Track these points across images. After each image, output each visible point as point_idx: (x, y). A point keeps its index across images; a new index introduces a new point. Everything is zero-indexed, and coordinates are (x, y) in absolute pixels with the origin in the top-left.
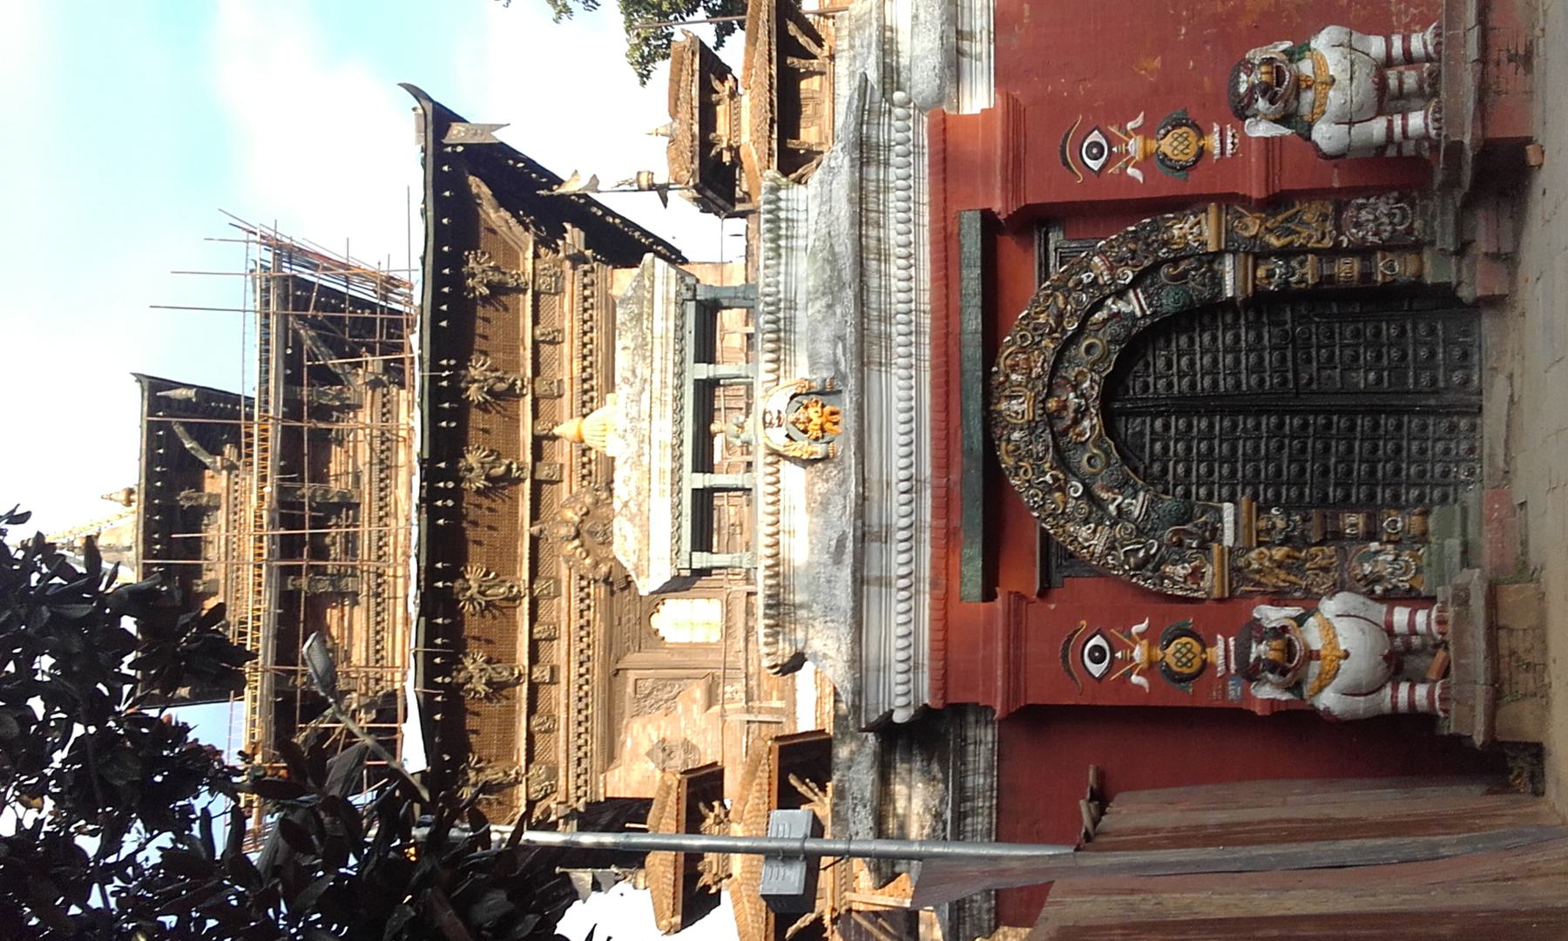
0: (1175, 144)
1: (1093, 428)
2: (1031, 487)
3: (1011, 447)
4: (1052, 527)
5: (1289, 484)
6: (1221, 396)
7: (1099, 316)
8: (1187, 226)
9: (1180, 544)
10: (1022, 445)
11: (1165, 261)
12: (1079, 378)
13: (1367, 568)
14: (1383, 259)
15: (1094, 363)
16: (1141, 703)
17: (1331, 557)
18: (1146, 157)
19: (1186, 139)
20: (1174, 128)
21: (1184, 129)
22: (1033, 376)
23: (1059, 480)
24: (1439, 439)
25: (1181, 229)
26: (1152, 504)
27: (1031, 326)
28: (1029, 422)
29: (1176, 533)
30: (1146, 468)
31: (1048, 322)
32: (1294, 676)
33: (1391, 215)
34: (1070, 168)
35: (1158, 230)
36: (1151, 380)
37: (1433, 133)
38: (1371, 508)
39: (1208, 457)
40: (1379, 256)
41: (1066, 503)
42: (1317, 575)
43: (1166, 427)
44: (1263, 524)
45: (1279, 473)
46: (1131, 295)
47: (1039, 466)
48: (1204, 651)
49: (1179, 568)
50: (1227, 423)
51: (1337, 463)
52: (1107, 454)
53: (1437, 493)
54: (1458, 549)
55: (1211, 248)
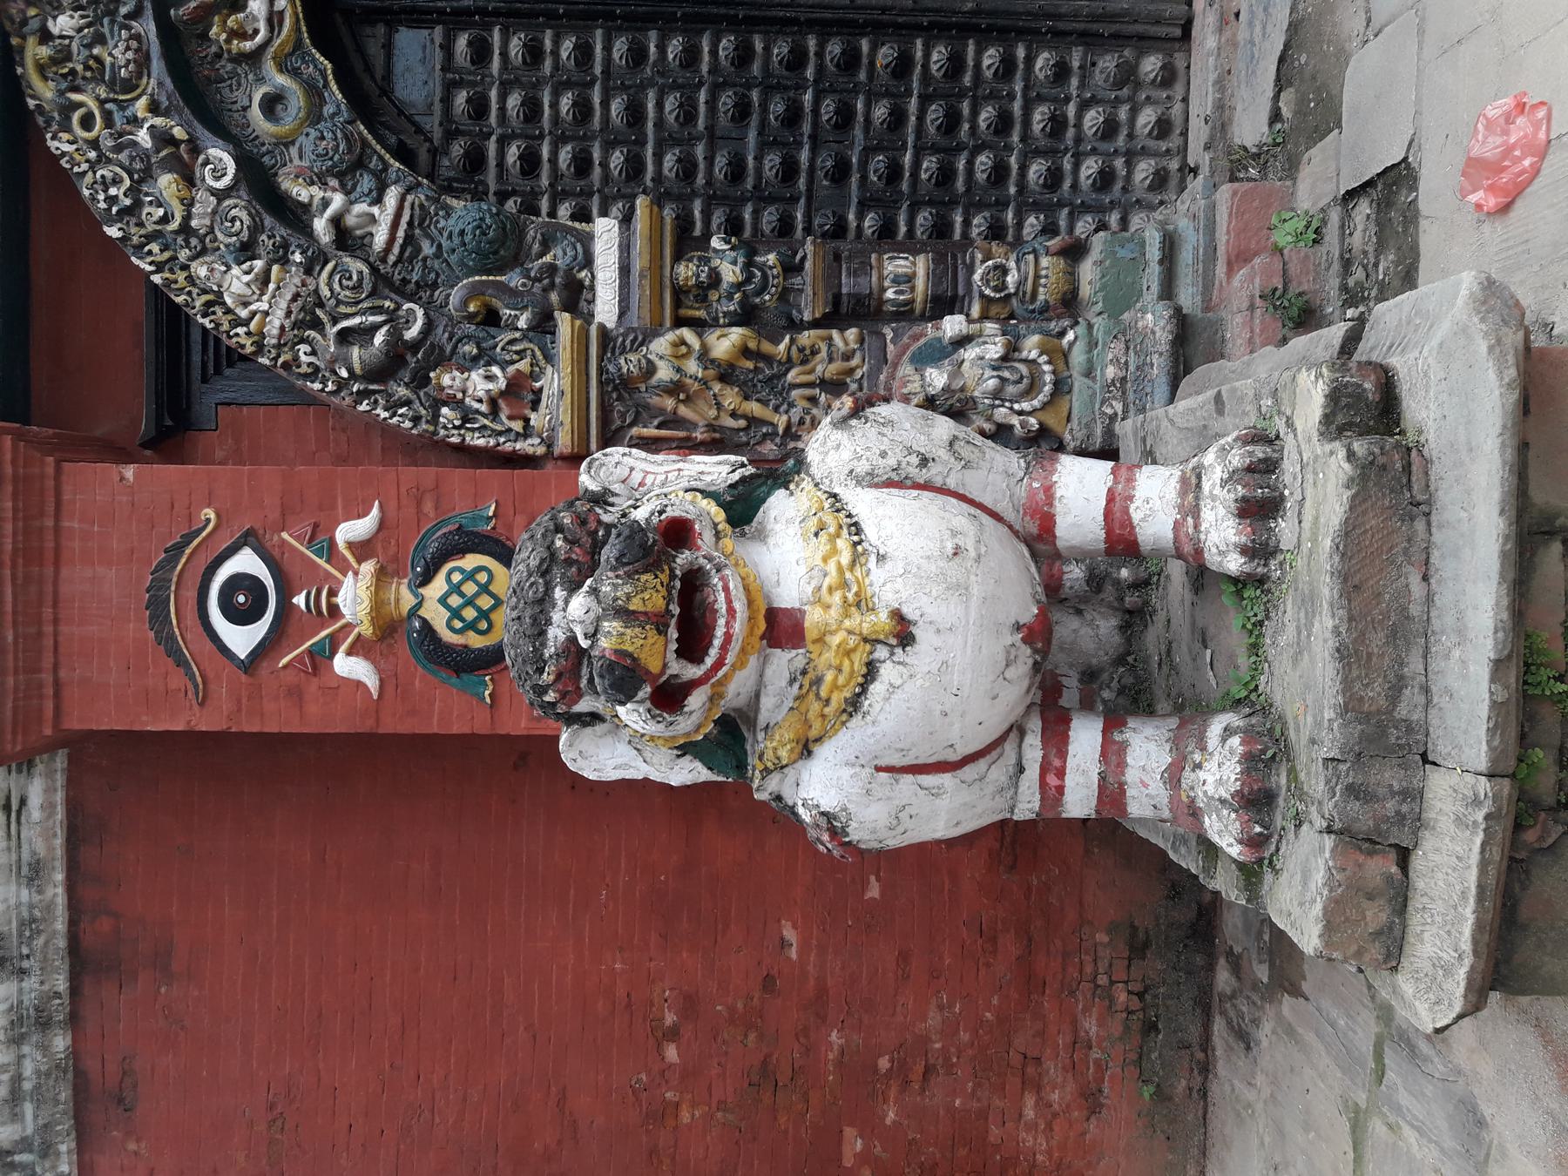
2: (102, 160)
3: (45, 52)
5: (762, 198)
9: (491, 318)
16: (366, 726)
17: (847, 357)
23: (173, 142)
29: (475, 292)
30: (434, 152)
32: (713, 699)
41: (189, 204)
42: (813, 400)
43: (481, 52)
44: (686, 271)
45: (737, 171)
51: (868, 152)
52: (315, 94)
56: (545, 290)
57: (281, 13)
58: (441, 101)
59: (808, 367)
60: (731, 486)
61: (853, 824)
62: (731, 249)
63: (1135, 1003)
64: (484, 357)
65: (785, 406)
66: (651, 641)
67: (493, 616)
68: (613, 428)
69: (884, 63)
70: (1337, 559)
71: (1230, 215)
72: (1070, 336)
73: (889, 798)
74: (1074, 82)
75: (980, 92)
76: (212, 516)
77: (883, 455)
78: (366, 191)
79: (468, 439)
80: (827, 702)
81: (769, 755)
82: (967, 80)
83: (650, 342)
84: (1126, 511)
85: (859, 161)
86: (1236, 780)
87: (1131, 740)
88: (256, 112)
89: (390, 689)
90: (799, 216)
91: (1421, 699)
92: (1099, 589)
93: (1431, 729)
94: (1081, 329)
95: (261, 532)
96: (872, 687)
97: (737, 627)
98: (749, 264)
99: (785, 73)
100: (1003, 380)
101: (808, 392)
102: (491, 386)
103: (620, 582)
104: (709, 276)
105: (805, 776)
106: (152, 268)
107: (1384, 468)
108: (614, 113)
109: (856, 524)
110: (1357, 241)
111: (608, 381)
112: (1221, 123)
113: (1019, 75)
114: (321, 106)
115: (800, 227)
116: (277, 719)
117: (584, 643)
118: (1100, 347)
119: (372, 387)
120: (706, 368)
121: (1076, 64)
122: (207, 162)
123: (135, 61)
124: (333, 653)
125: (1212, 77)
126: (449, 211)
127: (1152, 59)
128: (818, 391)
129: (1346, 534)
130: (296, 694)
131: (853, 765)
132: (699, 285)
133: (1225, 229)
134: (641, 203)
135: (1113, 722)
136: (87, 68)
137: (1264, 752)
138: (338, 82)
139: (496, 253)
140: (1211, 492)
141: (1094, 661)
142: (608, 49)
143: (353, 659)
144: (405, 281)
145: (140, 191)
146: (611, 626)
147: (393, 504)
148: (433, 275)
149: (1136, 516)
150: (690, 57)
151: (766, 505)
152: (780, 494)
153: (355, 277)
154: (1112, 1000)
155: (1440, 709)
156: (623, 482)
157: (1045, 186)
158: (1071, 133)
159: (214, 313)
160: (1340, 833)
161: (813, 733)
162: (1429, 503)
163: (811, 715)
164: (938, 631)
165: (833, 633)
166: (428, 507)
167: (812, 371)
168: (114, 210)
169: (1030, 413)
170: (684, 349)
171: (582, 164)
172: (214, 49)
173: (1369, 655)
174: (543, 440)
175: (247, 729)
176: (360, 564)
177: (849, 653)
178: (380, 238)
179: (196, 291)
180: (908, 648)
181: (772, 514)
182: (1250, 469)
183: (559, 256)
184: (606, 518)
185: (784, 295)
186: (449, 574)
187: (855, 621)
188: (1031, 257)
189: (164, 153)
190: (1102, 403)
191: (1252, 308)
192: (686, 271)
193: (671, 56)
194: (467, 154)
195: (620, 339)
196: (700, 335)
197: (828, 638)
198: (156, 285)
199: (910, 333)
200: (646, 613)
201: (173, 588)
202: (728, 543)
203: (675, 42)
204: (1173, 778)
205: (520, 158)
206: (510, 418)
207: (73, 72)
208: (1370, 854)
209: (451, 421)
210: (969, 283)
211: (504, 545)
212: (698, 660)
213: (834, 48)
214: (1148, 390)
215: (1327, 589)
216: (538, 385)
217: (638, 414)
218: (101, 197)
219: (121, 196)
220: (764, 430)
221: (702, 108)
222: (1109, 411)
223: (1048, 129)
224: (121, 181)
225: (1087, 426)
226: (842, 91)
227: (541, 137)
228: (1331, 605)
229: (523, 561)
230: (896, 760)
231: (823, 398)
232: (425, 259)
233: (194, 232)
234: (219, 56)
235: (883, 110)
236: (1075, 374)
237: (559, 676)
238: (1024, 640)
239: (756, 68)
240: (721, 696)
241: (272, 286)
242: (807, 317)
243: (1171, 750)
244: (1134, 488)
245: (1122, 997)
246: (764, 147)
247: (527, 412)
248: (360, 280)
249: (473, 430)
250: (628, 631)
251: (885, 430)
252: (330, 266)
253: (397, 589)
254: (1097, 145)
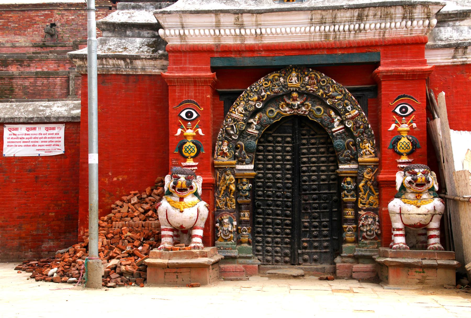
0: (405, 144)
1: (285, 112)
2: (260, 87)
3: (276, 77)
4: (243, 96)
6: (299, 165)
7: (333, 113)
8: (370, 149)
9: (237, 148)
10: (278, 82)
11: (355, 141)
12: (306, 106)
13: (226, 221)
14: (353, 228)
15: (312, 112)
17: (231, 207)
18: (399, 132)
19: (407, 148)
20: (412, 143)
21: (411, 147)
22: (307, 86)
24: (281, 249)
25: (368, 146)
26: (252, 136)
27: (328, 85)
28: (288, 85)
30: (271, 134)
31: (329, 91)
33: (370, 231)
34: (395, 101)
35: (368, 137)
36: (307, 137)
37: (395, 246)
38: (253, 222)
39: (274, 159)
40: (355, 226)
41: (253, 101)
42: (224, 201)
43: (288, 142)
44: (245, 180)
45: (269, 187)
46: (341, 127)
47: (269, 89)
48: (192, 157)
49: (226, 147)
50: (288, 166)
52: (274, 118)
53: (259, 248)
54: (233, 255)
55: (360, 159)
56: (241, 157)
57: (286, 113)
67: (187, 153)
72: (233, 241)
74: (285, 246)
82: (284, 227)
94: (234, 243)
101: (225, 201)
102: (225, 150)
122: (260, 103)
124: (182, 129)
136: (274, 84)
144: (244, 133)
146: (181, 183)
150: (288, 179)
158: (276, 245)
171: (269, 160)
178: (250, 130)
185: (241, 196)
188: (248, 236)
192: (245, 180)
207: (274, 81)
210: (244, 226)
213: (289, 204)
233: (248, 101)
241: (240, 115)
242: (238, 200)
252: (244, 123)
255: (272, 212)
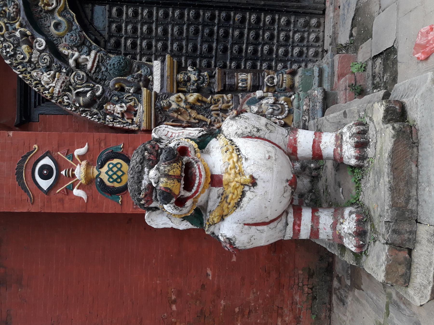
2: (5, 40)
5: (202, 57)
9: (122, 89)
16: (83, 210)
17: (228, 102)
23: (26, 35)
29: (117, 82)
30: (105, 42)
32: (194, 203)
41: (31, 54)
42: (218, 115)
43: (120, 13)
44: (181, 77)
45: (195, 49)
51: (233, 44)
52: (70, 23)
56: (139, 81)
58: (108, 27)
59: (216, 105)
60: (199, 137)
61: (237, 242)
62: (194, 71)
63: (310, 291)
64: (120, 101)
65: (210, 116)
66: (176, 184)
67: (122, 178)
68: (159, 122)
69: (238, 19)
70: (390, 160)
71: (339, 63)
72: (293, 97)
73: (248, 234)
74: (292, 26)
75: (265, 28)
76: (37, 147)
77: (246, 128)
78: (85, 52)
79: (115, 125)
80: (229, 204)
81: (211, 220)
82: (261, 24)
83: (170, 97)
84: (319, 146)
85: (230, 47)
86: (355, 227)
87: (321, 215)
88: (52, 28)
89: (90, 199)
90: (213, 62)
91: (415, 203)
92: (304, 170)
93: (419, 212)
94: (296, 95)
95: (52, 152)
96: (243, 199)
97: (203, 180)
98: (199, 75)
99: (209, 21)
100: (274, 109)
101: (216, 112)
102: (122, 109)
103: (166, 166)
104: (187, 78)
105: (222, 227)
106: (19, 73)
107: (404, 132)
108: (159, 32)
109: (238, 149)
110: (377, 70)
111: (157, 108)
112: (334, 38)
113: (276, 23)
114: (72, 27)
115: (213, 65)
116: (56, 208)
117: (154, 185)
118: (302, 100)
119: (86, 109)
120: (186, 105)
121: (292, 21)
122: (37, 42)
123: (16, 12)
125: (332, 25)
126: (110, 58)
127: (314, 20)
128: (219, 112)
129: (393, 152)
130: (62, 201)
131: (237, 223)
132: (184, 81)
133: (337, 67)
134: (167, 56)
135: (315, 211)
137: (363, 219)
138: (77, 20)
139: (124, 70)
140: (346, 140)
141: (303, 191)
142: (157, 13)
143: (79, 190)
144: (96, 78)
145: (16, 50)
147: (92, 144)
148: (105, 77)
149: (322, 147)
150: (182, 16)
151: (209, 143)
152: (214, 140)
153: (81, 77)
154: (303, 290)
155: (422, 206)
156: (166, 135)
157: (283, 55)
158: (291, 40)
159: (38, 87)
160: (390, 244)
161: (225, 213)
162: (418, 143)
163: (224, 208)
164: (264, 182)
165: (231, 182)
166: (103, 145)
167: (218, 106)
168: (8, 55)
169: (281, 119)
170: (180, 99)
171: (149, 46)
172: (40, 9)
173: (400, 190)
174: (137, 125)
175: (46, 211)
176: (81, 161)
177: (236, 188)
178: (89, 65)
179: (33, 80)
180: (255, 187)
181: (212, 146)
182: (358, 133)
183: (143, 72)
184: (161, 146)
186: (109, 165)
187: (238, 179)
188: (281, 75)
189: (24, 39)
190: (302, 117)
191: (346, 89)
192: (181, 77)
193: (176, 15)
194: (115, 42)
195: (161, 96)
196: (185, 95)
197: (230, 184)
198: (21, 78)
199: (246, 95)
200: (174, 176)
201: (24, 169)
202: (199, 154)
203: (177, 11)
204: (334, 226)
205: (131, 43)
206: (128, 119)
208: (400, 251)
209: (110, 120)
211: (125, 156)
212: (190, 191)
213: (223, 14)
214: (316, 113)
215: (386, 169)
216: (136, 109)
217: (166, 118)
218: (4, 51)
219: (10, 51)
220: (203, 123)
221: (185, 31)
222: (304, 119)
223: (285, 39)
224: (11, 47)
225: (298, 123)
226: (225, 27)
227: (137, 38)
228: (388, 174)
229: (135, 159)
230: (250, 222)
231: (221, 114)
232: (102, 72)
234: (41, 11)
235: (237, 32)
236: (295, 108)
237: (146, 195)
238: (289, 185)
239: (201, 20)
240: (196, 202)
241: (56, 79)
242: (216, 90)
243: (333, 218)
244: (321, 139)
245: (306, 289)
246: (202, 42)
247: (133, 117)
248: (83, 78)
249: (116, 122)
250: (169, 181)
251: (246, 121)
252: (74, 73)
253: (93, 169)
254: (298, 44)
255: (236, 44)
